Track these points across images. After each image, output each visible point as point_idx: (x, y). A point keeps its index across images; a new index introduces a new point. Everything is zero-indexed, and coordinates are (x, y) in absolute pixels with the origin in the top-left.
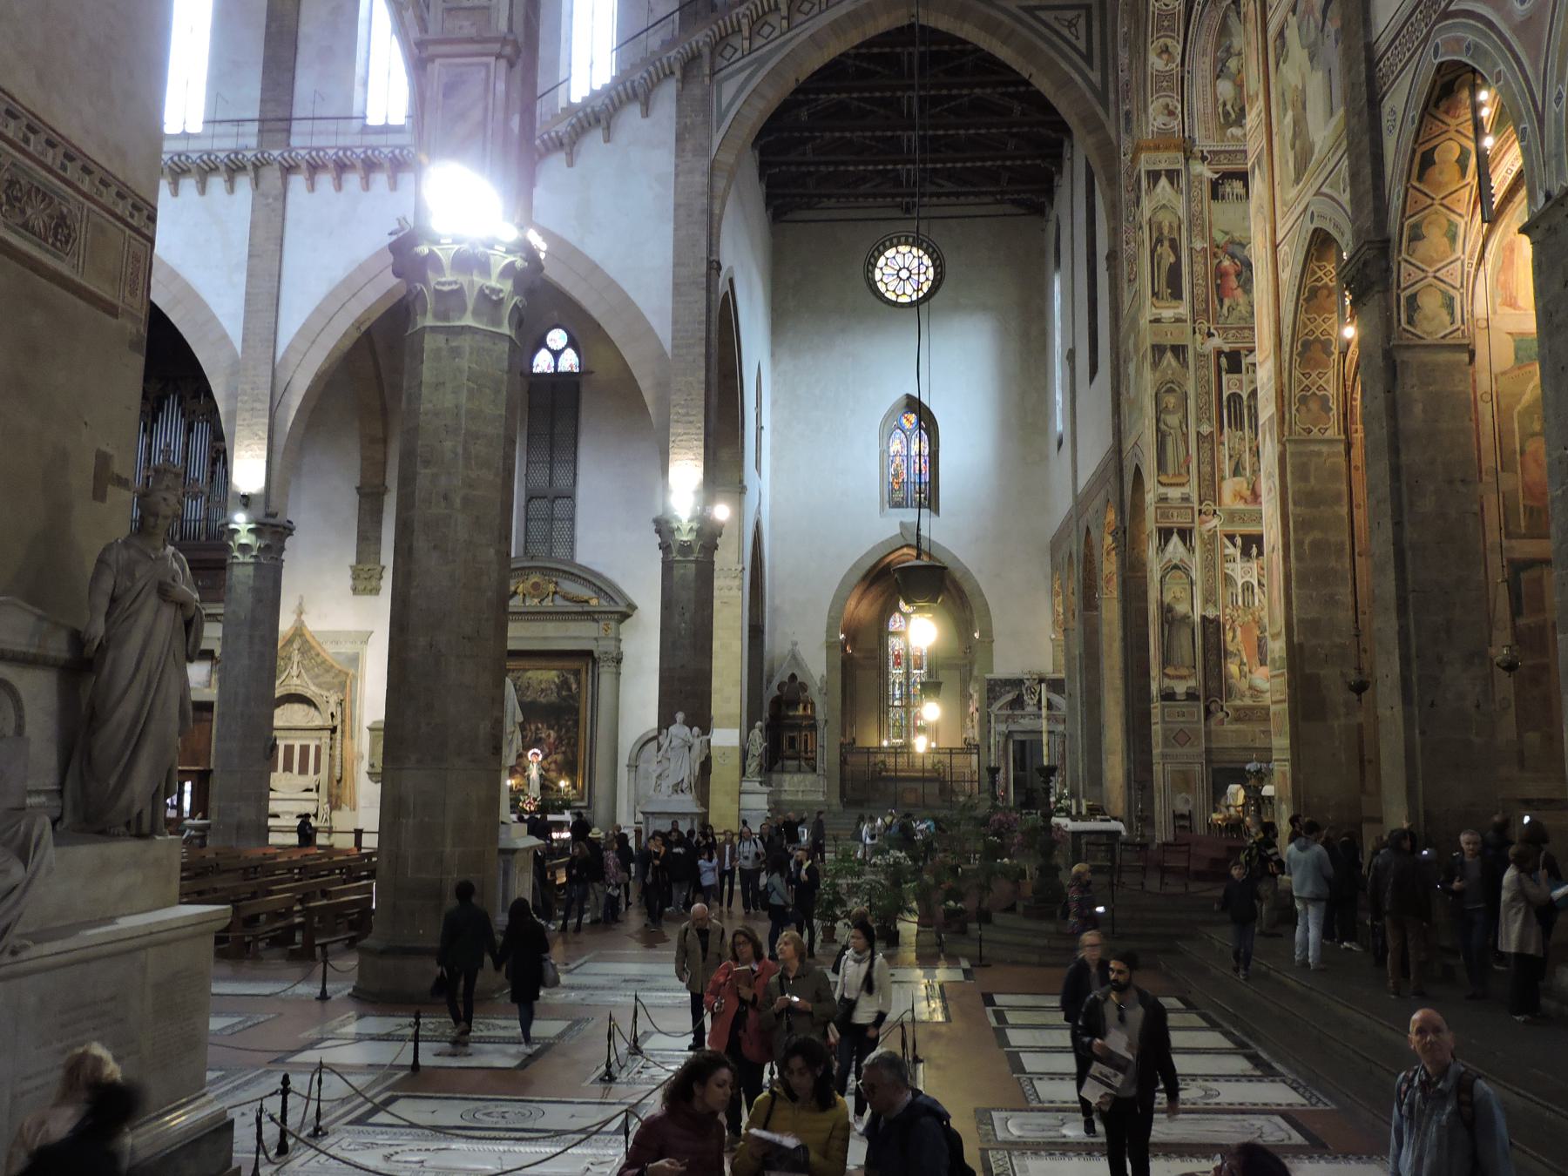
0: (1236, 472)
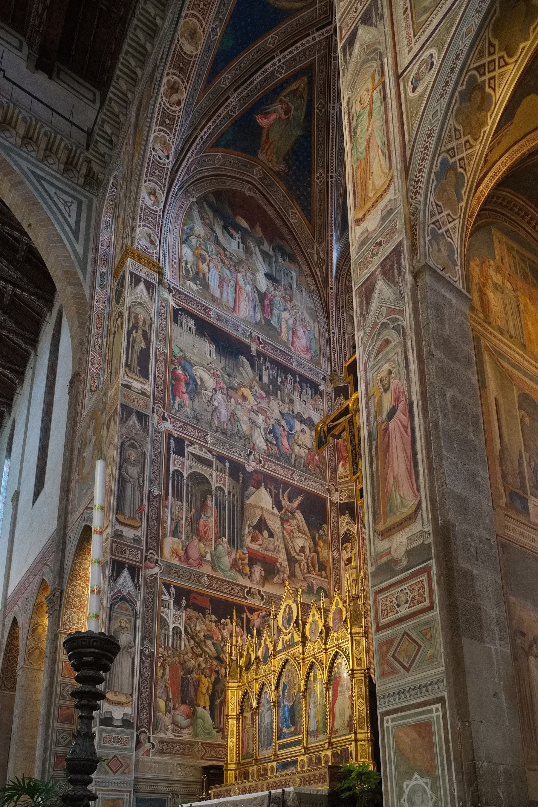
0: (175, 533)
